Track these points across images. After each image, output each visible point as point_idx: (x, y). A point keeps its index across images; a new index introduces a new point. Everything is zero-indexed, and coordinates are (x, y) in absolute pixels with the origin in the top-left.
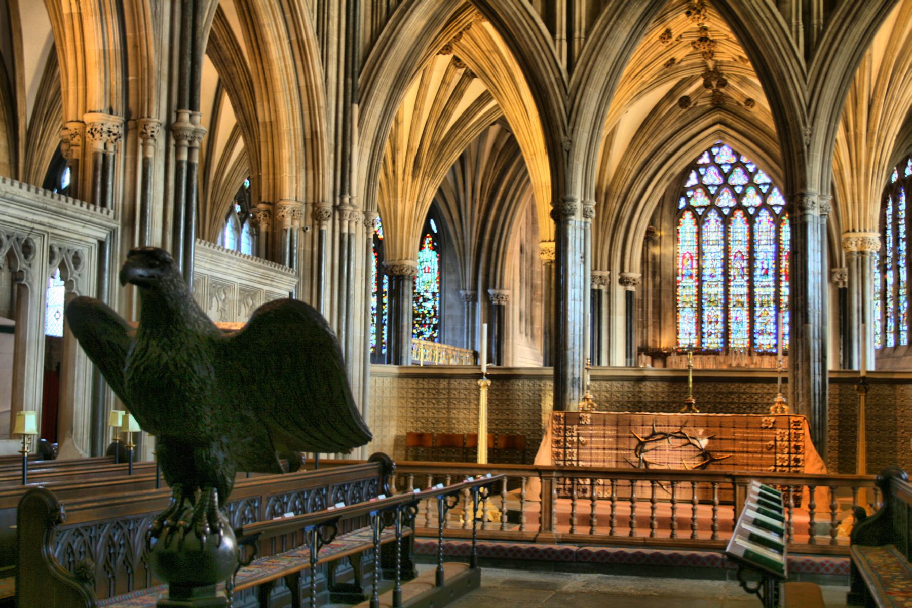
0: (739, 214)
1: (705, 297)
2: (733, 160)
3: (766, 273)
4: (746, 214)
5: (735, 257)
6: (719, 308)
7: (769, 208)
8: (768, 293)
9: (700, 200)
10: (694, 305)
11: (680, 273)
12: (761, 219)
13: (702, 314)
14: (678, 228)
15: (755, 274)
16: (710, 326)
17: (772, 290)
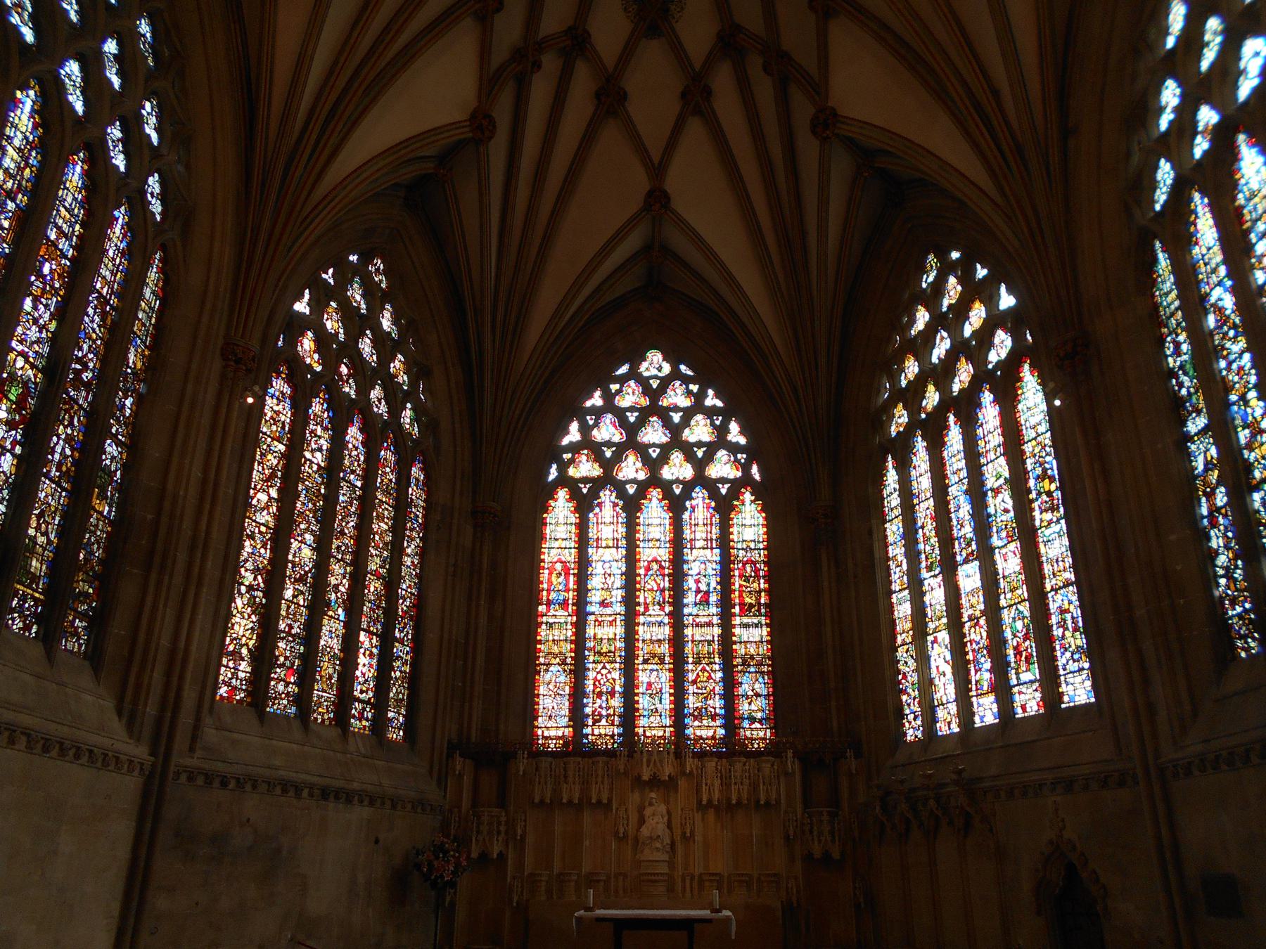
0: (655, 494)
1: (590, 644)
2: (645, 402)
3: (705, 601)
4: (667, 493)
5: (648, 569)
6: (617, 666)
7: (711, 486)
8: (709, 638)
9: (585, 468)
10: (569, 660)
11: (545, 598)
12: (694, 502)
13: (585, 678)
14: (545, 515)
15: (685, 601)
16: (598, 701)
17: (717, 631)
